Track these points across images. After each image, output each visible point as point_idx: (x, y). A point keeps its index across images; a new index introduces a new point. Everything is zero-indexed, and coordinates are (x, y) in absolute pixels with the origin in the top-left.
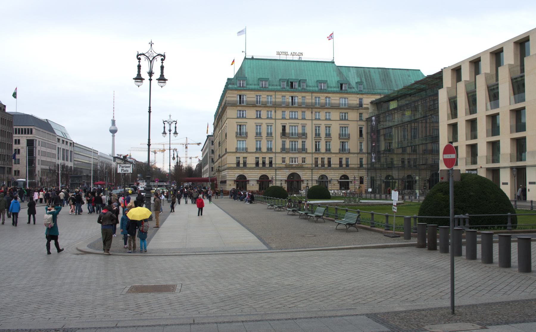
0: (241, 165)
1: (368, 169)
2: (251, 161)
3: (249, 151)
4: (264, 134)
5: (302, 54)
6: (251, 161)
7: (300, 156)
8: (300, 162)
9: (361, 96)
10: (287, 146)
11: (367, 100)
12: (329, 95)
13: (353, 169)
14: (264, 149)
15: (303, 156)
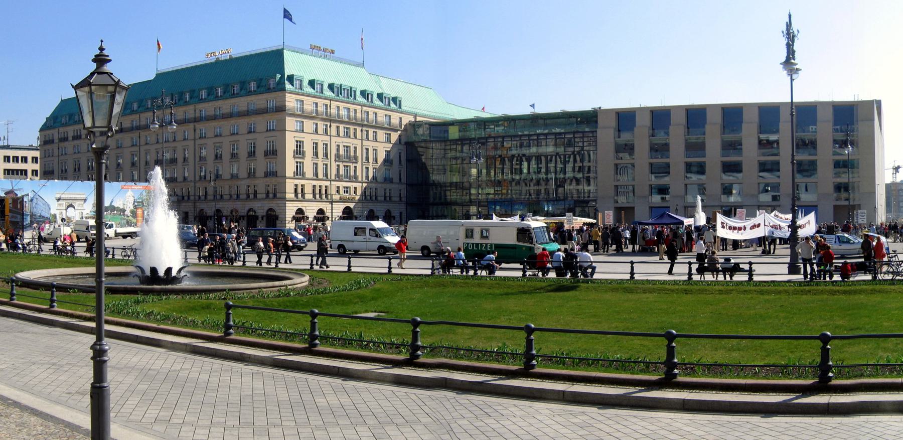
0: (299, 193)
1: (408, 204)
2: (308, 190)
3: (307, 176)
4: (320, 154)
5: (333, 52)
6: (308, 190)
7: (351, 185)
8: (352, 192)
9: (401, 115)
10: (342, 172)
11: (407, 119)
12: (377, 110)
13: (395, 202)
14: (320, 176)
15: (355, 185)
